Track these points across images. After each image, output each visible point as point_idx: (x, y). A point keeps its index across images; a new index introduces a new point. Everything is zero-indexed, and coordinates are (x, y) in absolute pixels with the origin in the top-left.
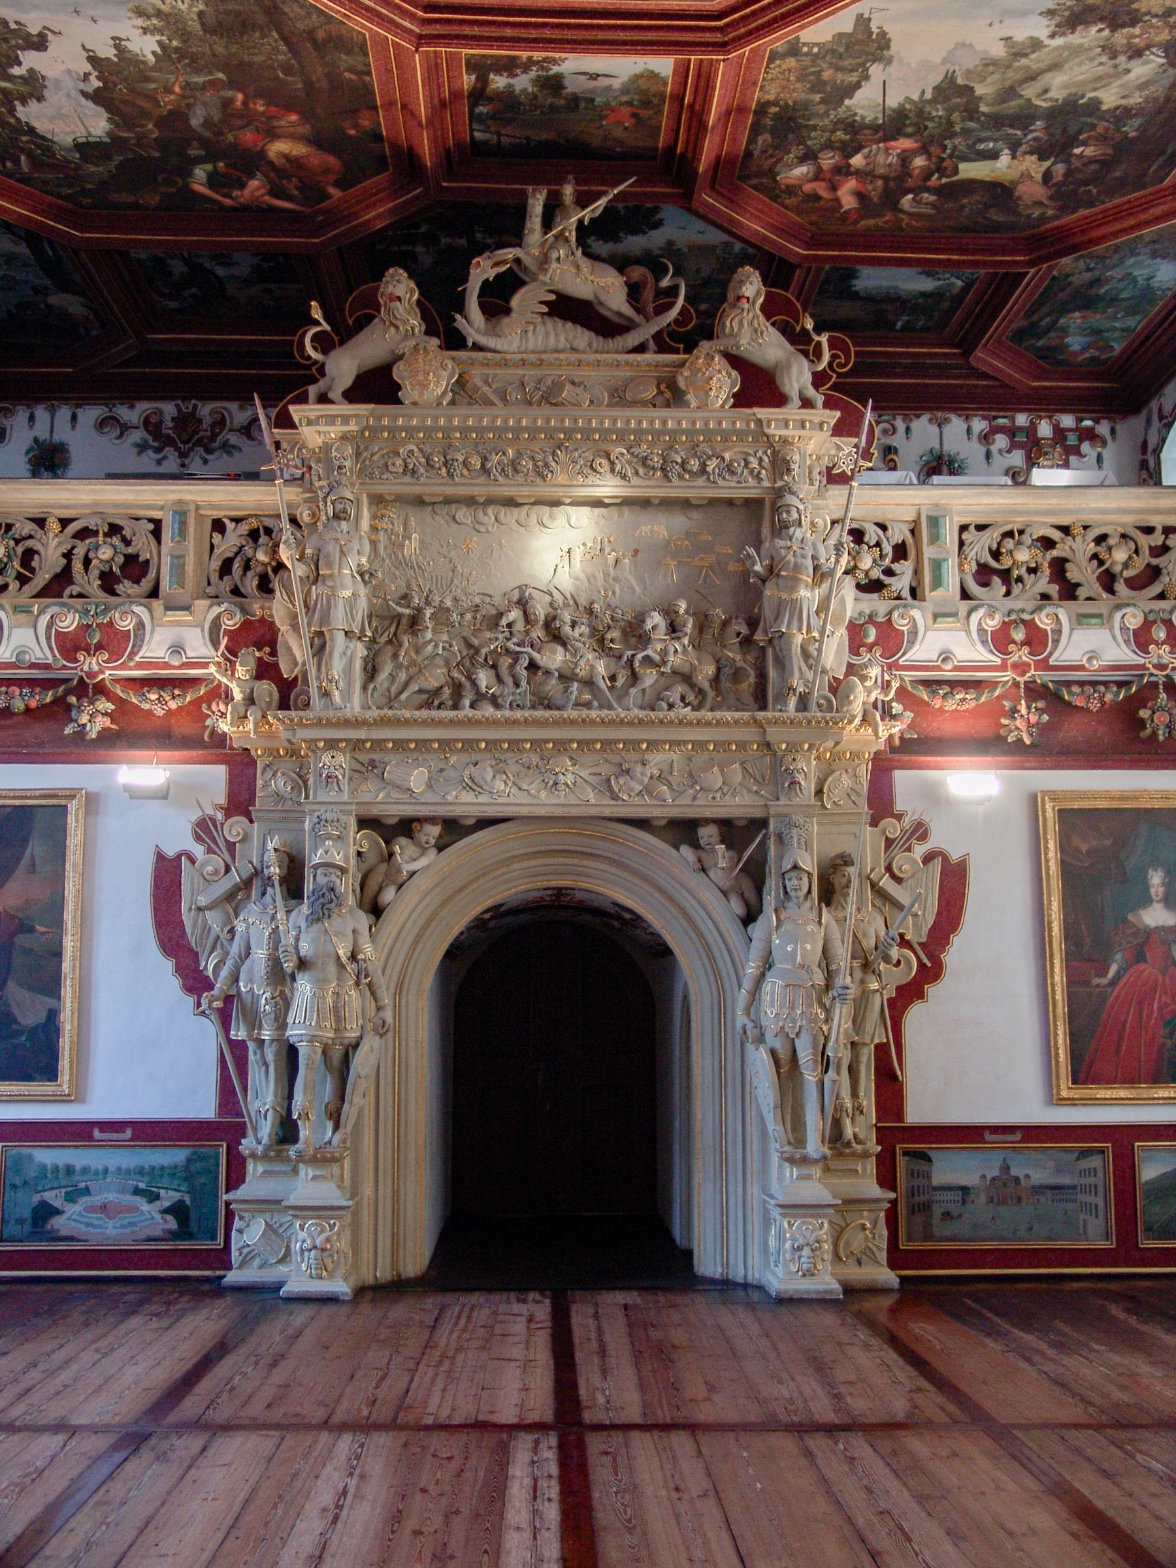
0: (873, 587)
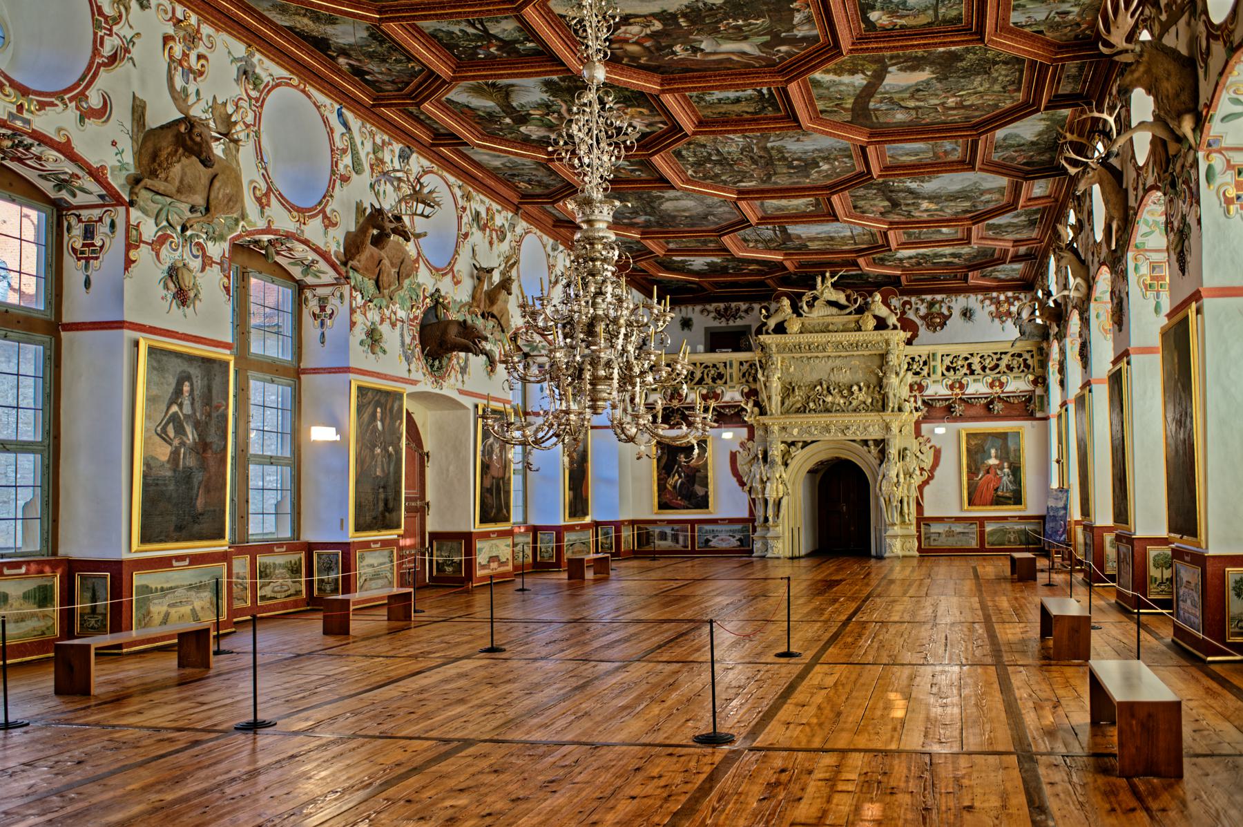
0: (917, 373)
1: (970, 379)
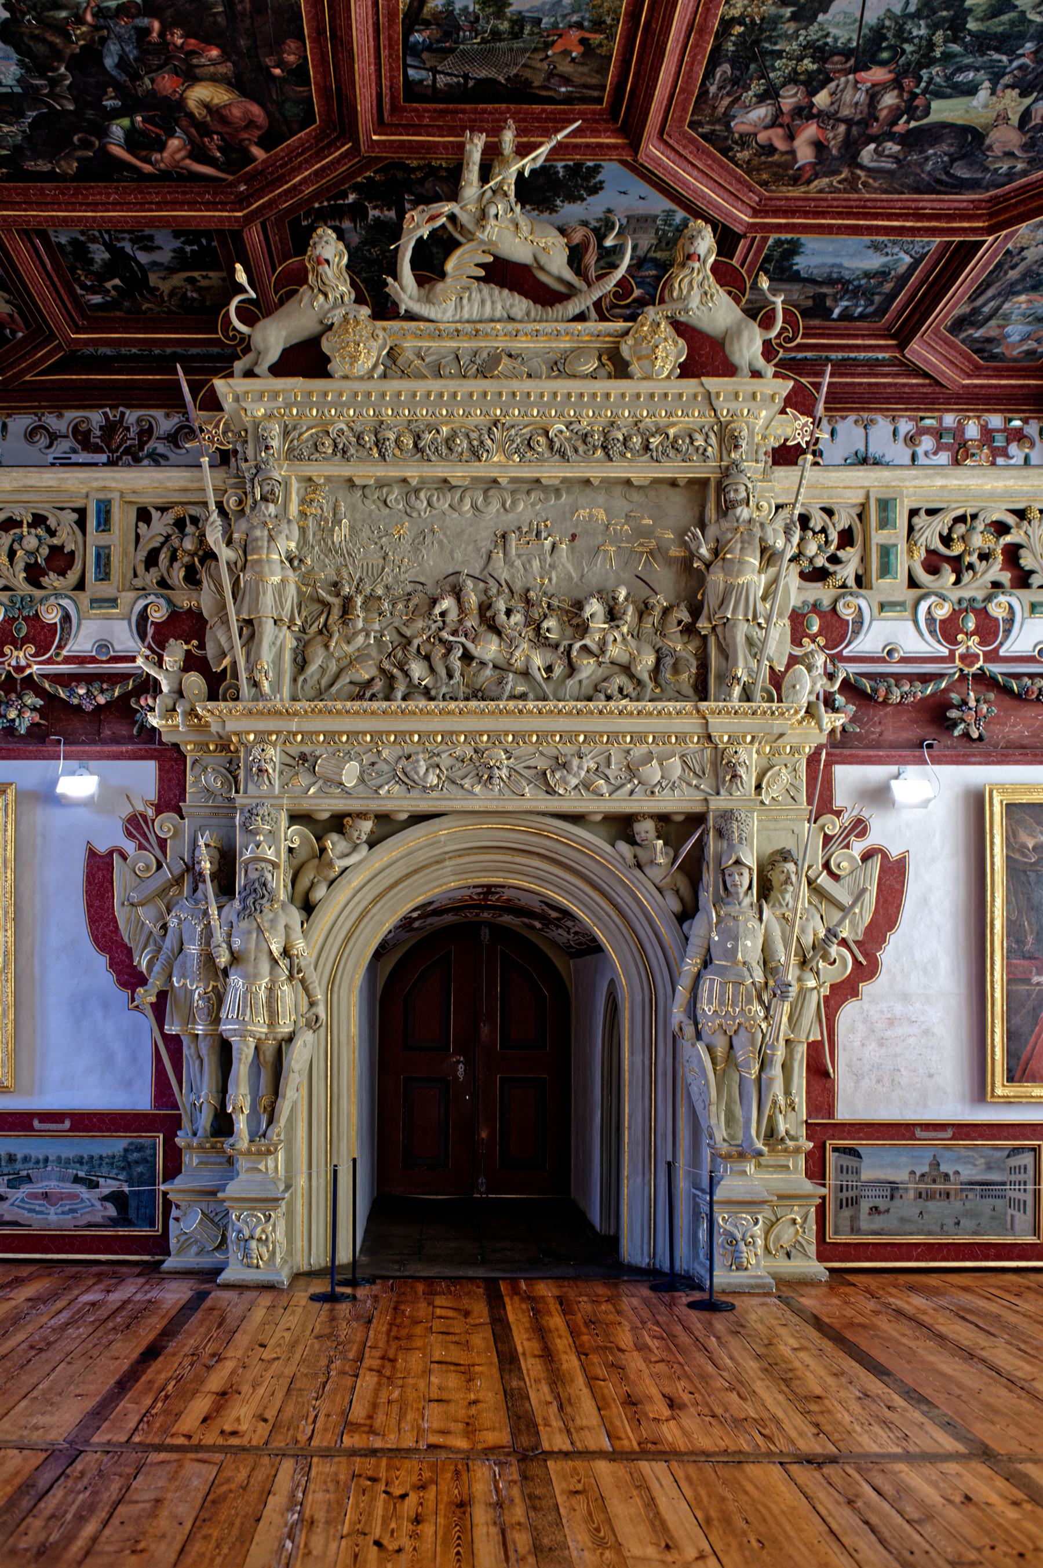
0: (818, 575)
1: (1016, 600)
